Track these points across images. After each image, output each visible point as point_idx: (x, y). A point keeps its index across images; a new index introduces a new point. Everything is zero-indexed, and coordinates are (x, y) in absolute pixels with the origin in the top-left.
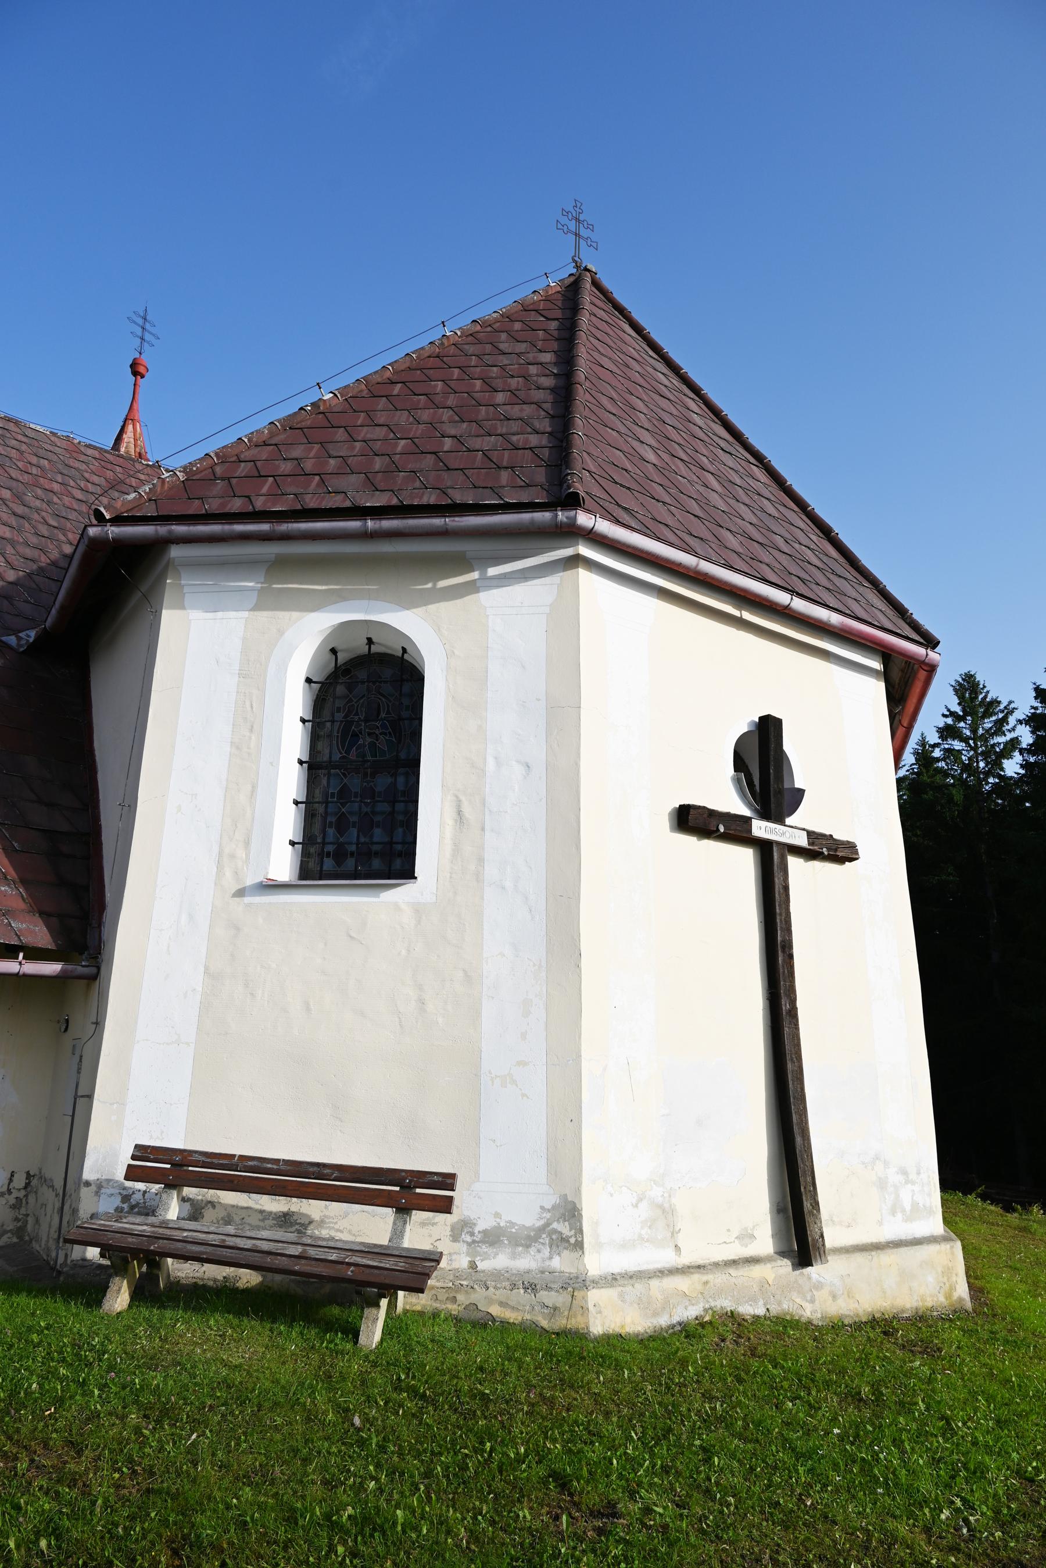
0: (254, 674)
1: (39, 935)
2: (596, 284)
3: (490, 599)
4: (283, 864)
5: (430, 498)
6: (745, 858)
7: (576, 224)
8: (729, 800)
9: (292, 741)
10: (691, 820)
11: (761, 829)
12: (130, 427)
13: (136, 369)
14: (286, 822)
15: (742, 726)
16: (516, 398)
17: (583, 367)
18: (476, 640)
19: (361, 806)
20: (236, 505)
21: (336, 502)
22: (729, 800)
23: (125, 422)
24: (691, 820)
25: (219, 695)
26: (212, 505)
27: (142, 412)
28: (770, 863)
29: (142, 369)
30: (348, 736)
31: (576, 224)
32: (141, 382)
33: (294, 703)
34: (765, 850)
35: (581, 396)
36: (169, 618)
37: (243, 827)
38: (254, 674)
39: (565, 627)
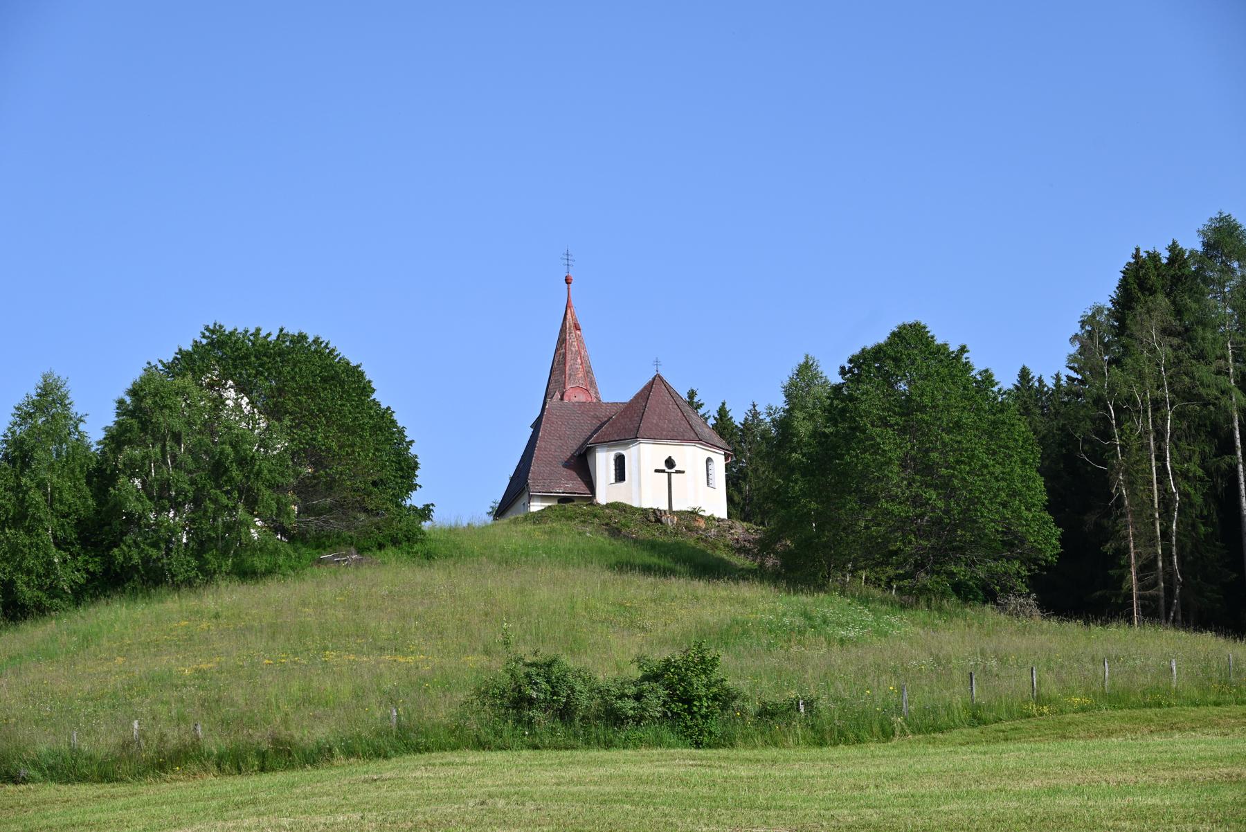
0: (607, 460)
4: (613, 481)
7: (657, 363)
8: (664, 467)
9: (613, 467)
10: (657, 471)
13: (568, 281)
18: (630, 453)
22: (664, 467)
24: (657, 471)
25: (604, 461)
27: (573, 303)
28: (669, 474)
31: (657, 363)
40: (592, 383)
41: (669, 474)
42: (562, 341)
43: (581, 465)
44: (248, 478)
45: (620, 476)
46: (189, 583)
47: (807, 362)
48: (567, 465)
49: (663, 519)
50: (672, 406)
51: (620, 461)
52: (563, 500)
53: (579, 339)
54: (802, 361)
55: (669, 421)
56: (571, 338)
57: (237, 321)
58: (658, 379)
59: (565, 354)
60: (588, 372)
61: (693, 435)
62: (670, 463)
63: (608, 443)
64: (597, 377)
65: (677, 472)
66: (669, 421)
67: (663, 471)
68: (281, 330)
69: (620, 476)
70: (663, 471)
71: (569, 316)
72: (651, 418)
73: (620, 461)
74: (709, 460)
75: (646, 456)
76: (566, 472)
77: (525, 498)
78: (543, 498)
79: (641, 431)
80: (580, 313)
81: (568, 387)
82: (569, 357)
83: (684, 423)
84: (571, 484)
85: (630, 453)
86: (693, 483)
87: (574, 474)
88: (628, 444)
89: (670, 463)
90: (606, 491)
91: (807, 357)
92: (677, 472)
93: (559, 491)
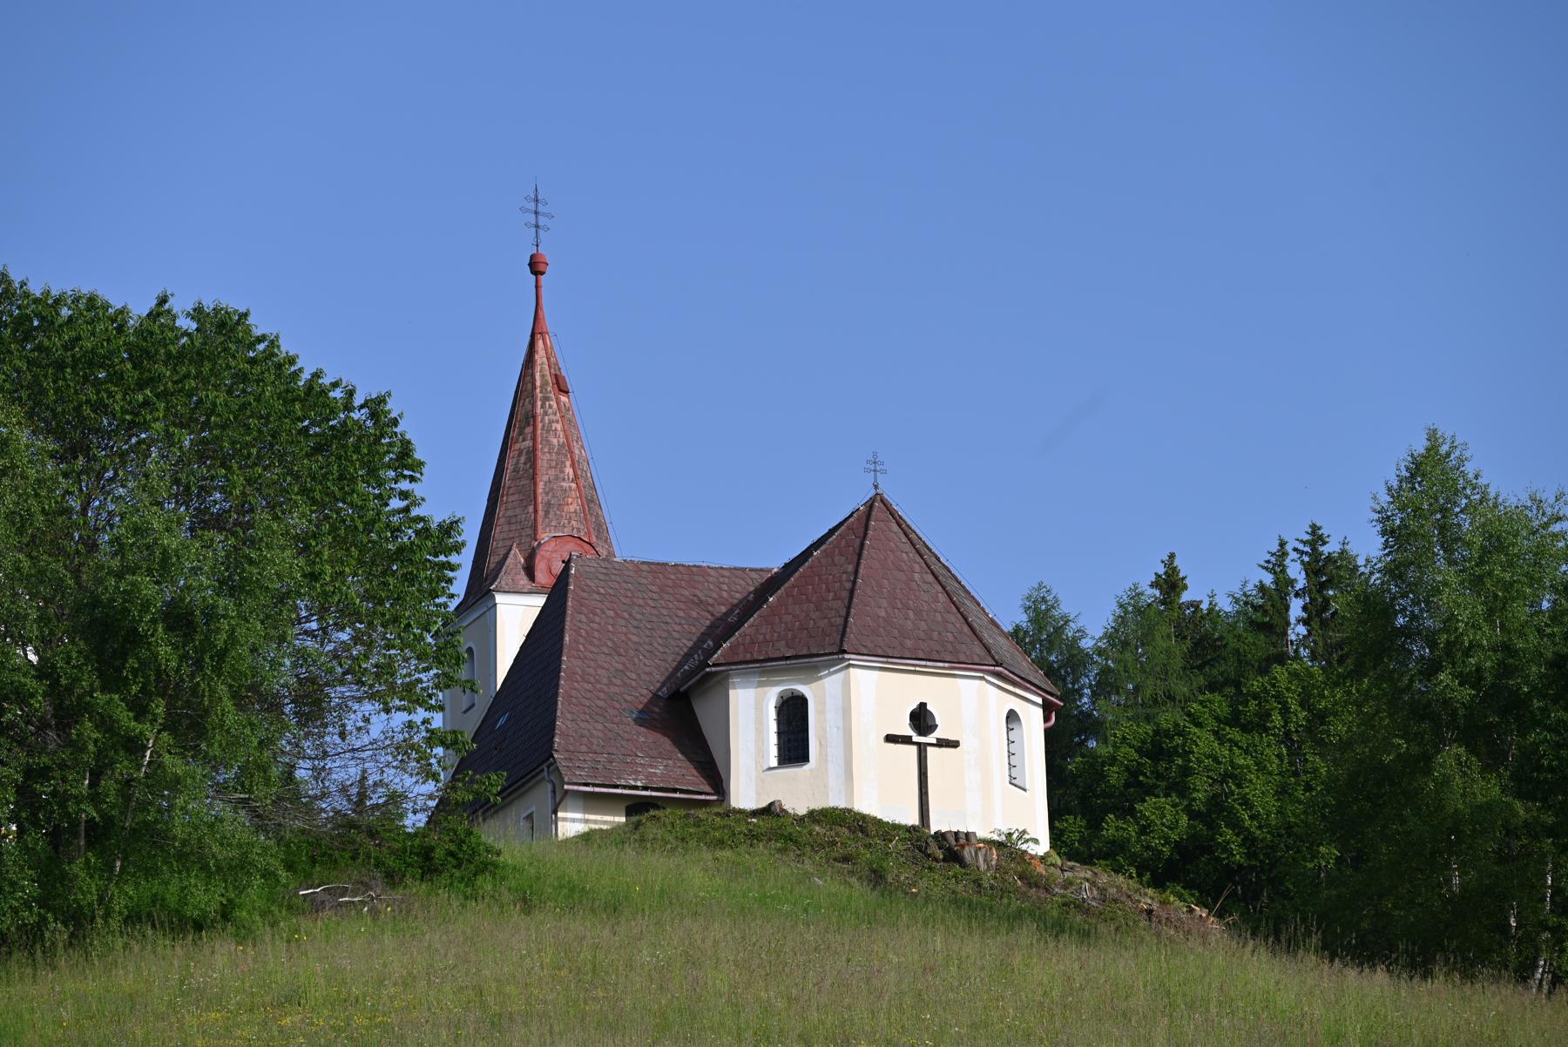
0: (759, 707)
1: (708, 789)
3: (827, 681)
4: (774, 762)
5: (805, 652)
6: (914, 749)
7: (875, 465)
9: (773, 727)
10: (891, 739)
11: (916, 738)
12: (540, 343)
13: (536, 267)
14: (774, 751)
18: (821, 694)
19: (794, 744)
20: (748, 657)
23: (533, 335)
24: (891, 739)
25: (750, 713)
26: (741, 658)
27: (549, 322)
28: (922, 748)
29: (541, 268)
30: (789, 723)
31: (875, 465)
32: (542, 278)
33: (772, 714)
34: (919, 744)
36: (731, 692)
37: (761, 753)
38: (759, 707)
39: (847, 685)
40: (601, 528)
41: (922, 748)
42: (521, 417)
43: (682, 717)
44: (199, 665)
45: (794, 747)
46: (33, 936)
47: (1432, 449)
48: (646, 718)
49: (967, 853)
50: (920, 576)
51: (793, 716)
52: (636, 807)
53: (564, 412)
54: (1420, 447)
55: (918, 613)
56: (548, 410)
59: (532, 454)
60: (590, 503)
61: (979, 650)
62: (922, 719)
63: (762, 665)
64: (611, 512)
65: (942, 743)
66: (918, 613)
67: (906, 740)
68: (163, 301)
69: (794, 747)
70: (906, 740)
71: (540, 357)
72: (872, 607)
73: (793, 716)
74: (1012, 717)
75: (863, 701)
76: (645, 736)
77: (540, 796)
78: (593, 801)
79: (851, 636)
80: (566, 348)
81: (544, 536)
82: (543, 460)
83: (954, 618)
84: (659, 767)
85: (821, 694)
86: (990, 773)
87: (666, 743)
88: (816, 668)
89: (922, 719)
91: (1432, 436)
92: (942, 743)
93: (635, 783)
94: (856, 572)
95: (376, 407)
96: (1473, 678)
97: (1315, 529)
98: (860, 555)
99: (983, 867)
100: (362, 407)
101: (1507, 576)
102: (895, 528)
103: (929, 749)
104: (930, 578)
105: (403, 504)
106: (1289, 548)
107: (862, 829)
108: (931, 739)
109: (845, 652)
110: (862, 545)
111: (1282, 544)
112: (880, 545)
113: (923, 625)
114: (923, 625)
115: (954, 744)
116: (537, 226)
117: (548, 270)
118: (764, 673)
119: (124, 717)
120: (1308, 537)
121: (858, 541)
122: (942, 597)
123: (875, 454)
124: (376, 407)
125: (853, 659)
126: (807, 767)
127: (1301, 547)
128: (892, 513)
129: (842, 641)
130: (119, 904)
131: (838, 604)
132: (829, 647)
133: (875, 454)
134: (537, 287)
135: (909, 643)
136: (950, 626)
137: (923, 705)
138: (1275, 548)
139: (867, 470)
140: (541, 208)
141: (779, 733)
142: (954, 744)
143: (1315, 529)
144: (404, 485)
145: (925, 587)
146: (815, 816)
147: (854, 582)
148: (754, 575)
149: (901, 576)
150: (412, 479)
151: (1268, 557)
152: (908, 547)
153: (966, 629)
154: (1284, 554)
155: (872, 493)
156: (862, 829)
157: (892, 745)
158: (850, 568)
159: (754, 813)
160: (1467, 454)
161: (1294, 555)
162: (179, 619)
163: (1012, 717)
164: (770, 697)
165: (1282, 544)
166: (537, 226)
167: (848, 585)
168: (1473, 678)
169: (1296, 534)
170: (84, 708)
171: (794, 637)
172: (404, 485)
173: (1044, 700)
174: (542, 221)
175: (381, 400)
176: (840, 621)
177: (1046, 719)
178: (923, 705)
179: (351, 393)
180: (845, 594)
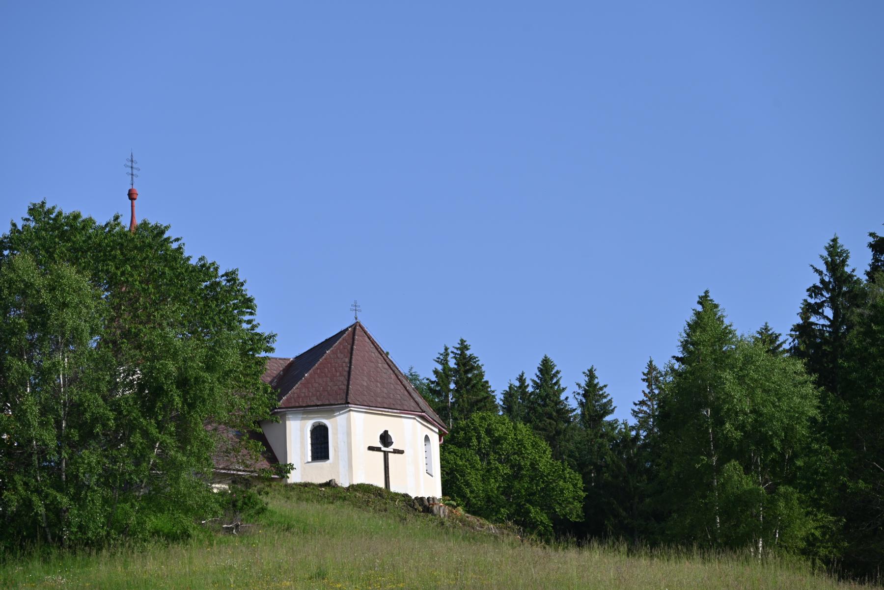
0: (302, 430)
2: (360, 326)
3: (338, 418)
4: (310, 459)
5: (327, 403)
6: (382, 454)
7: (356, 307)
8: (379, 445)
10: (371, 448)
13: (131, 196)
15: (382, 432)
16: (341, 375)
17: (353, 362)
18: (335, 424)
20: (297, 405)
21: (312, 404)
22: (379, 445)
24: (371, 448)
25: (297, 434)
26: (293, 405)
28: (386, 454)
31: (356, 307)
32: (135, 202)
34: (384, 452)
35: (352, 373)
36: (288, 422)
37: (303, 454)
38: (302, 430)
39: (349, 420)
50: (382, 365)
55: (382, 383)
57: (65, 205)
58: (356, 328)
61: (413, 404)
62: (385, 439)
63: (304, 408)
65: (396, 451)
66: (382, 383)
67: (379, 449)
72: (359, 381)
74: (427, 438)
85: (335, 424)
88: (333, 411)
89: (385, 439)
90: (302, 468)
92: (396, 451)
94: (350, 362)
95: (231, 276)
96: (741, 427)
97: (462, 341)
98: (351, 354)
99: (442, 516)
100: (223, 276)
101: (756, 376)
102: (367, 340)
103: (390, 454)
104: (386, 366)
105: (249, 326)
106: (449, 351)
107: (380, 495)
108: (390, 449)
109: (348, 403)
110: (352, 349)
111: (446, 349)
112: (361, 348)
113: (385, 391)
114: (385, 391)
115: (402, 452)
116: (132, 175)
117: (138, 198)
118: (305, 413)
119: (154, 431)
120: (458, 346)
121: (349, 347)
122: (393, 376)
123: (355, 302)
124: (231, 276)
125: (352, 407)
126: (328, 462)
127: (455, 351)
128: (365, 332)
129: (347, 398)
130: (149, 526)
131: (342, 378)
132: (341, 400)
133: (355, 302)
134: (132, 206)
135: (379, 400)
136: (398, 392)
137: (386, 432)
138: (442, 351)
139: (351, 310)
140: (134, 165)
141: (312, 444)
142: (402, 452)
143: (462, 341)
144: (247, 317)
145: (385, 371)
146: (354, 488)
147: (350, 367)
148: (281, 362)
149: (372, 364)
150: (251, 314)
151: (439, 356)
152: (374, 350)
153: (406, 393)
154: (447, 354)
155: (354, 321)
156: (380, 495)
157: (371, 452)
158: (347, 360)
159: (321, 485)
160: (724, 314)
161: (451, 355)
162: (183, 383)
163: (427, 438)
164: (309, 424)
165: (446, 349)
166: (132, 175)
167: (347, 369)
168: (741, 427)
169: (453, 344)
170: (132, 427)
171: (321, 395)
172: (247, 317)
173: (440, 430)
174: (135, 172)
175: (233, 273)
176: (344, 387)
177: (440, 440)
178: (386, 432)
179: (216, 269)
180: (346, 374)
